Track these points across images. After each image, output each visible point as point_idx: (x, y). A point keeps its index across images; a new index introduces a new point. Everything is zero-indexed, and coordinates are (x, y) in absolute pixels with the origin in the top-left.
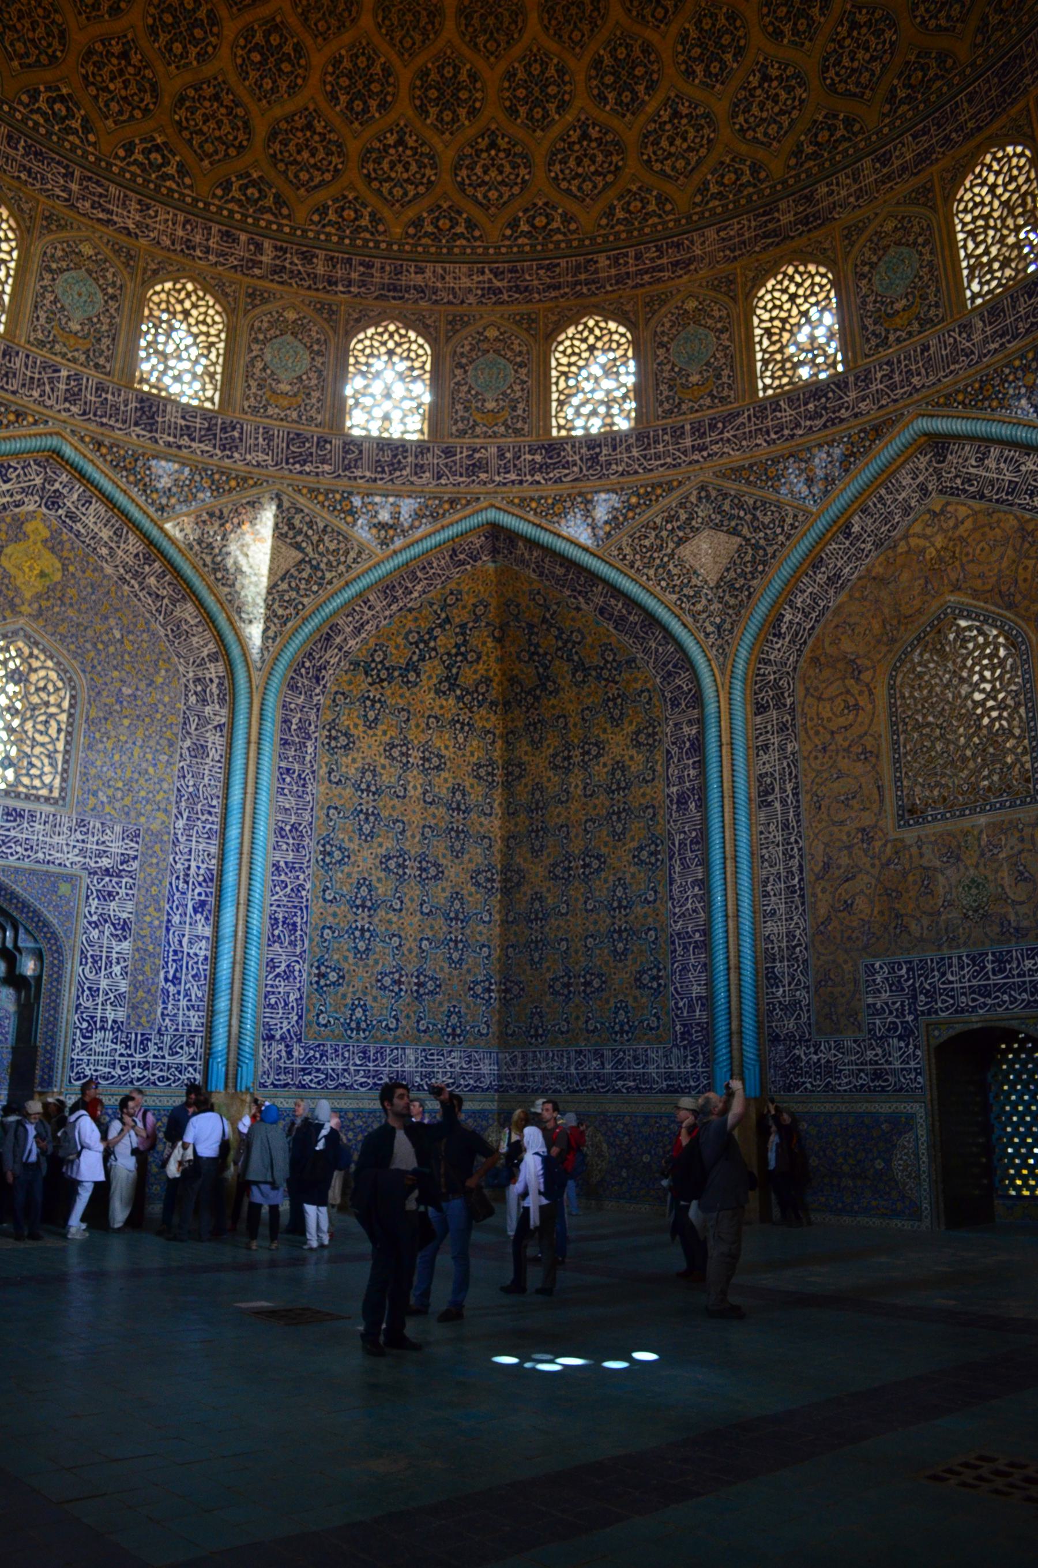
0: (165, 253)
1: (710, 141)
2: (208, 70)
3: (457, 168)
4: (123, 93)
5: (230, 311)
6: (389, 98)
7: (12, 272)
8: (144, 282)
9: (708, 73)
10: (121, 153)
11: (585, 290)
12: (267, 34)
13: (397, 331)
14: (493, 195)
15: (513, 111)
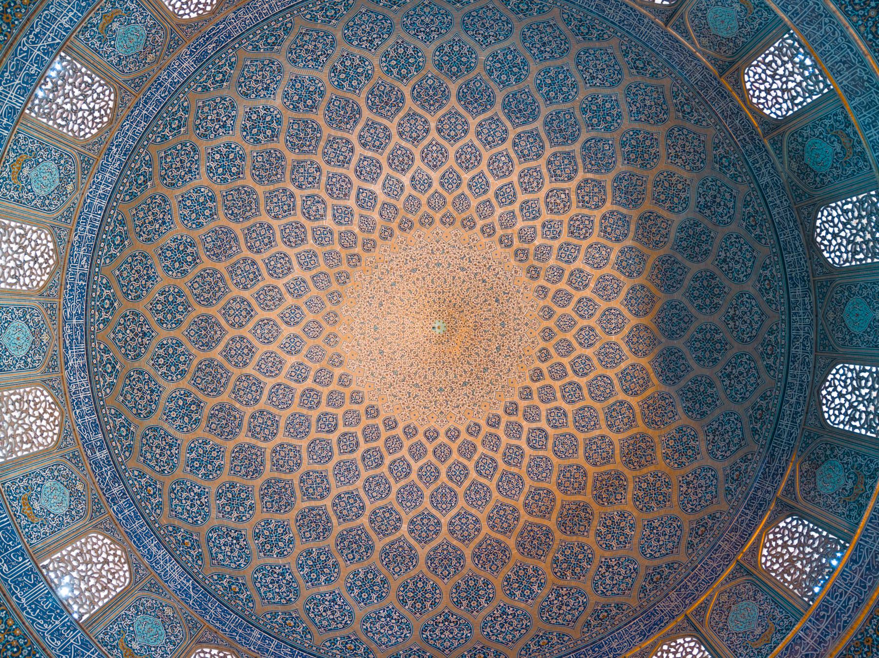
0: (67, 390)
1: (346, 623)
2: (161, 381)
3: (213, 530)
4: (128, 339)
5: (58, 446)
6: (211, 477)
7: (14, 287)
8: (44, 381)
9: (360, 595)
10: (102, 346)
11: (237, 638)
12: (193, 403)
13: (120, 557)
14: (220, 556)
15: (257, 536)
